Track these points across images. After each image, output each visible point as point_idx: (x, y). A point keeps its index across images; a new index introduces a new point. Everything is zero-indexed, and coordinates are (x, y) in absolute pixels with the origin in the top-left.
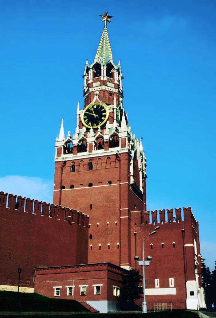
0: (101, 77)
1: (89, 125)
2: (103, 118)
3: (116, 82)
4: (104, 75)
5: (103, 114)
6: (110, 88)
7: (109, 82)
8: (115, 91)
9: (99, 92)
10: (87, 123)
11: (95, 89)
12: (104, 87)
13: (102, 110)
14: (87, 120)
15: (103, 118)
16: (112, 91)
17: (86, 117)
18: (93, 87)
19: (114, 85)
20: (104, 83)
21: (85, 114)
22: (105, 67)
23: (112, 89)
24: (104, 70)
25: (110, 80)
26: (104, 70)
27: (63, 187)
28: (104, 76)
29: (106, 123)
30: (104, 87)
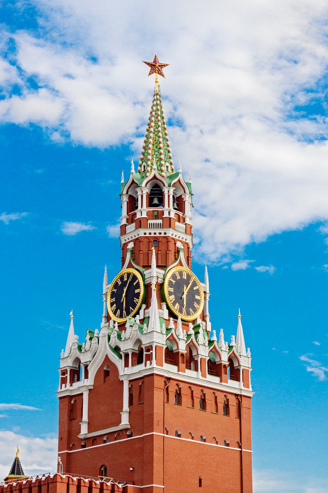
0: (136, 211)
1: (117, 315)
3: (166, 215)
5: (137, 291)
6: (152, 231)
7: (153, 219)
8: (165, 234)
9: (134, 244)
10: (115, 313)
12: (141, 233)
13: (134, 284)
14: (115, 305)
16: (158, 235)
19: (160, 221)
23: (157, 231)
24: (142, 196)
25: (156, 214)
26: (142, 196)
27: (74, 447)
29: (140, 308)
30: (141, 233)
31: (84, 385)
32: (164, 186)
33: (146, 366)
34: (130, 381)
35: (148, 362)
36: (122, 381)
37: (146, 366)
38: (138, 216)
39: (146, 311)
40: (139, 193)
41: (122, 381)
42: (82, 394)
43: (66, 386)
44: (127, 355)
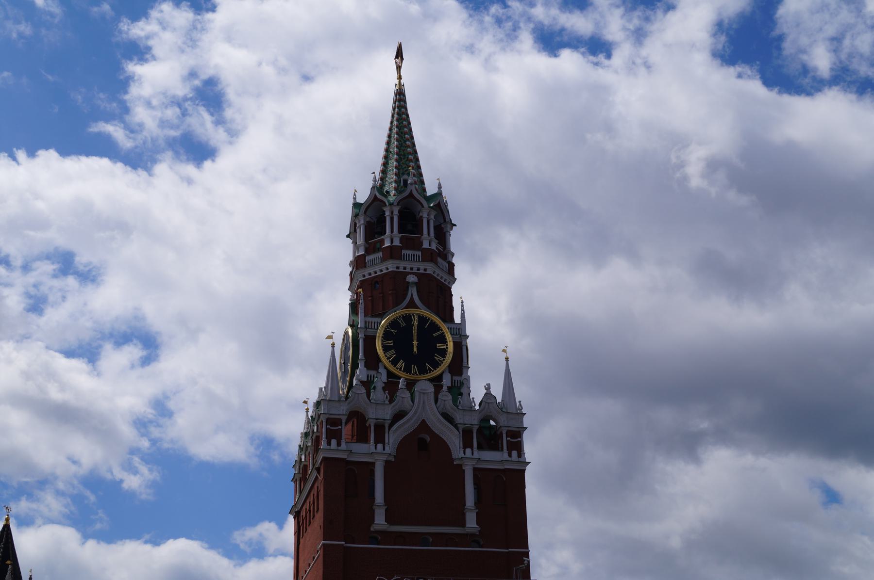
1: (398, 366)
2: (438, 358)
4: (429, 234)
5: (439, 346)
10: (394, 362)
11: (405, 268)
12: (430, 268)
15: (438, 358)
17: (390, 343)
18: (400, 257)
19: (447, 265)
20: (429, 256)
21: (387, 336)
22: (432, 217)
23: (446, 276)
28: (428, 242)
30: (430, 268)
31: (376, 454)
32: (445, 221)
33: (510, 455)
34: (475, 470)
35: (514, 453)
36: (460, 466)
37: (510, 455)
38: (426, 245)
39: (456, 378)
40: (425, 215)
41: (460, 466)
42: (373, 464)
43: (339, 444)
44: (467, 434)
